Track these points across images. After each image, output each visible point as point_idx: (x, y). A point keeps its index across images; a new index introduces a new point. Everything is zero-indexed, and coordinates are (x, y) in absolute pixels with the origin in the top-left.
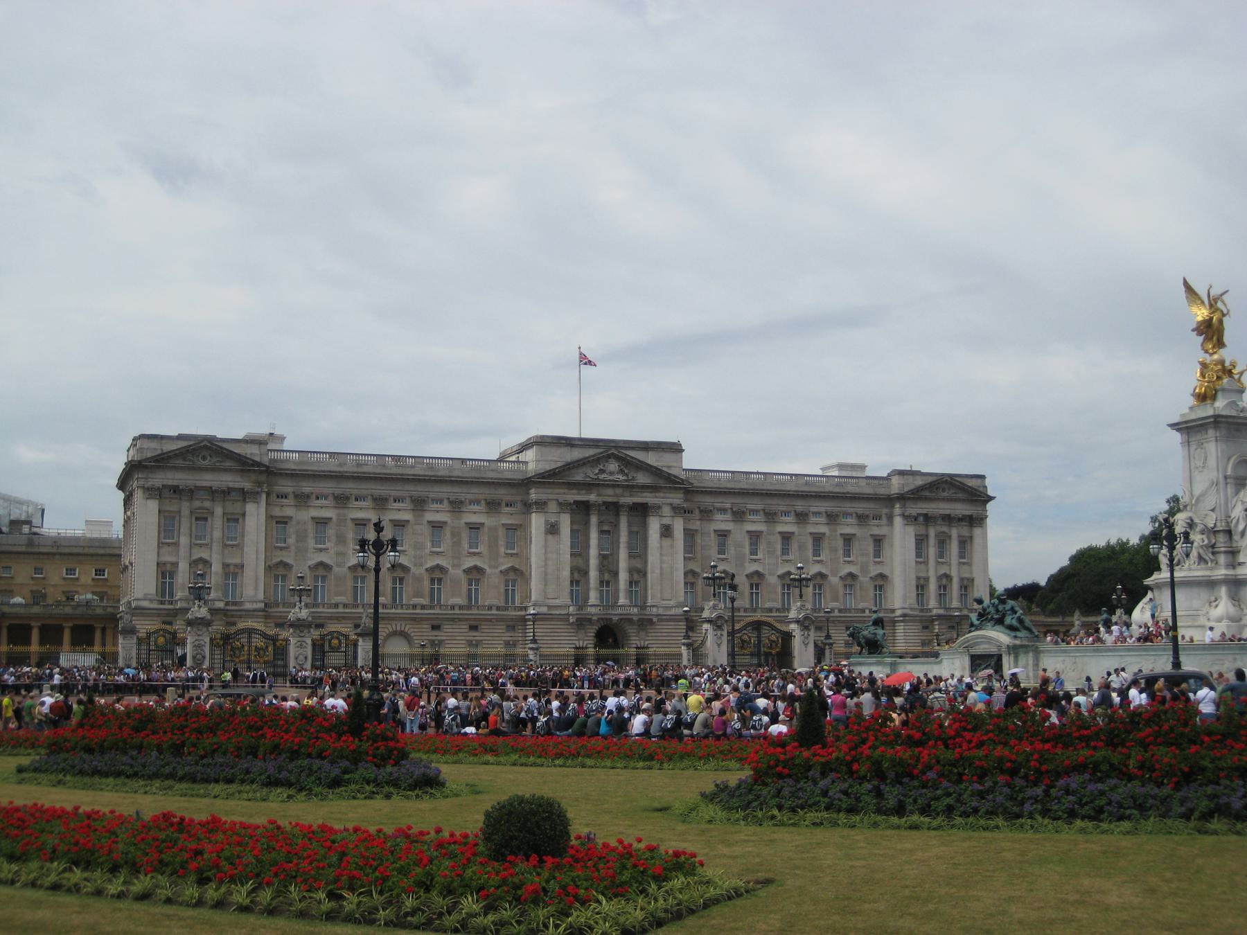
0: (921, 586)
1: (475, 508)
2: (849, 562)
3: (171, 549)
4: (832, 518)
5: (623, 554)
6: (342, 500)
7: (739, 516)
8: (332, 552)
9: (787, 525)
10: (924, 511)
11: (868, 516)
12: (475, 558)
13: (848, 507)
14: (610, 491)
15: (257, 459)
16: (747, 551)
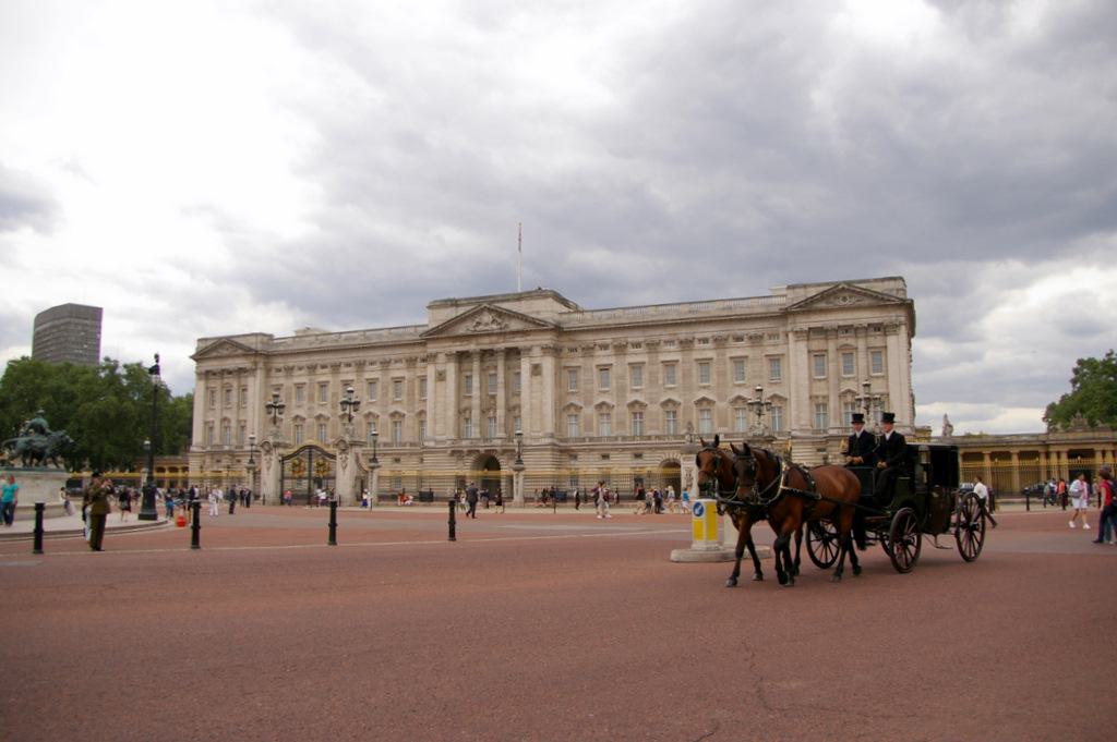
0: (820, 404)
1: (398, 365)
2: (739, 386)
3: (212, 412)
4: (720, 342)
5: (501, 394)
6: (312, 368)
7: (620, 349)
8: (306, 408)
9: (671, 353)
10: (819, 325)
11: (761, 337)
12: (399, 405)
13: (738, 329)
14: (486, 340)
15: (253, 347)
16: (628, 381)
